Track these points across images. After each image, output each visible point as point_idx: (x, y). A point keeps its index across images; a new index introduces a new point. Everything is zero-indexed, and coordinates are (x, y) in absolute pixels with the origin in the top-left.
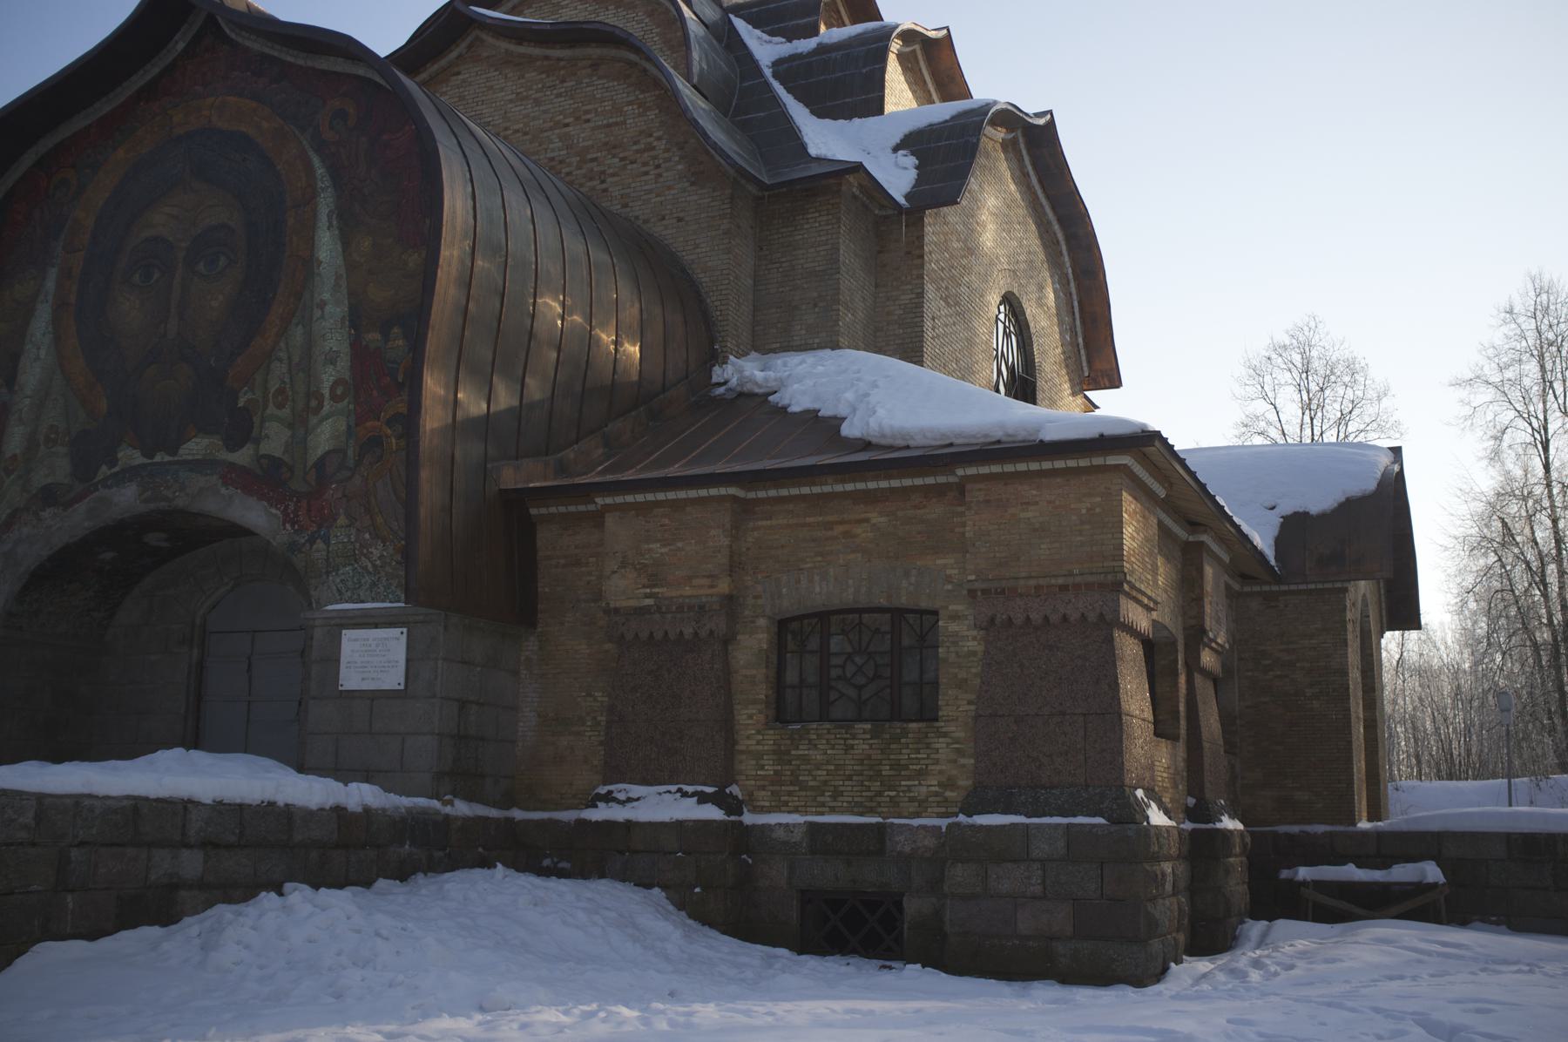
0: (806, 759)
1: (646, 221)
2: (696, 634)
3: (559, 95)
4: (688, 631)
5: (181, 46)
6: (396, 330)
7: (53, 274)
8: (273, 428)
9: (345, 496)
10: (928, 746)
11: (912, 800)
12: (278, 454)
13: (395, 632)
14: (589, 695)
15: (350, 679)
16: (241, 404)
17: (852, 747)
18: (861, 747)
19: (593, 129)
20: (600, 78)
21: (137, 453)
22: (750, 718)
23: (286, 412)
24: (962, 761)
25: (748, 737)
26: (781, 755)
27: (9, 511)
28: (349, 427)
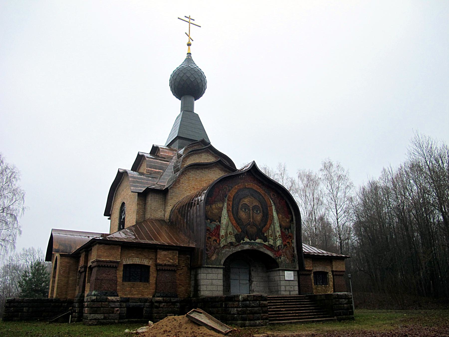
0: (318, 289)
8: (270, 240)
13: (292, 272)
15: (286, 279)
21: (248, 240)
23: (272, 238)
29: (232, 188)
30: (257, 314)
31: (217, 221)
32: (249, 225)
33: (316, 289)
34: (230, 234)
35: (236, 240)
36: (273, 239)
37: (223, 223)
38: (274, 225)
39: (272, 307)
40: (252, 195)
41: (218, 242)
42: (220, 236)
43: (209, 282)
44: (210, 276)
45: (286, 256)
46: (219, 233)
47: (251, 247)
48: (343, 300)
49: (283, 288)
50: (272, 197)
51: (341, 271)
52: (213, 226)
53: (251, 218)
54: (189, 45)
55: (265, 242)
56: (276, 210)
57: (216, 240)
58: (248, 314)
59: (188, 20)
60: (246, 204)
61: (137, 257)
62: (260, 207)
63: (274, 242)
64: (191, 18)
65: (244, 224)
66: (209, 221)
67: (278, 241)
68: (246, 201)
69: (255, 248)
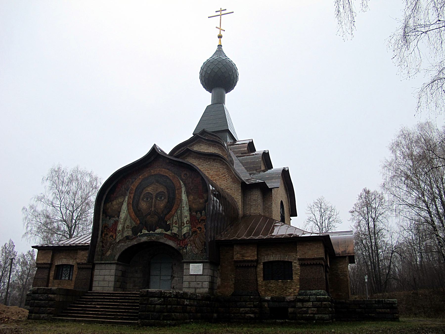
0: (270, 286)
1: (224, 189)
2: (251, 265)
3: (206, 165)
4: (249, 265)
5: (153, 159)
6: (198, 213)
7: (127, 197)
8: (174, 228)
9: (189, 241)
10: (291, 284)
11: (289, 293)
12: (176, 233)
13: (201, 264)
14: (230, 275)
16: (168, 223)
17: (278, 284)
18: (280, 284)
19: (214, 171)
20: (215, 162)
22: (260, 279)
23: (177, 225)
24: (297, 286)
25: (260, 283)
26: (266, 285)
28: (190, 229)
29: (136, 179)
30: (44, 307)
31: (116, 216)
32: (149, 215)
33: (266, 285)
34: (127, 227)
35: (133, 234)
36: (178, 227)
37: (121, 218)
38: (181, 210)
39: (94, 303)
40: (157, 182)
41: (114, 237)
42: (117, 231)
43: (101, 278)
44: (103, 272)
45: (194, 245)
46: (117, 228)
47: (149, 238)
48: (156, 299)
49: (186, 284)
50: (184, 178)
51: (314, 259)
52: (112, 221)
53: (153, 206)
54: (220, 37)
55: (166, 231)
56: (187, 192)
57: (112, 236)
58: (36, 307)
59: (219, 13)
60: (149, 193)
61: (65, 259)
62: (166, 193)
63: (179, 230)
64: (222, 9)
65: (144, 215)
66: (108, 217)
67: (185, 228)
68: (149, 189)
69: (154, 239)
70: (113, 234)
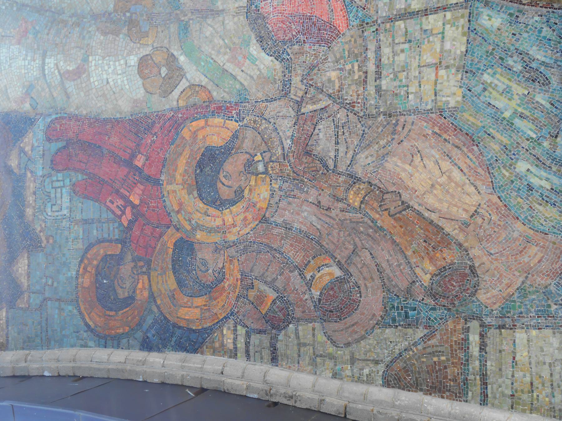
27: (255, 49)
31: (13, 163)
37: (29, 88)
70: (182, 164)
